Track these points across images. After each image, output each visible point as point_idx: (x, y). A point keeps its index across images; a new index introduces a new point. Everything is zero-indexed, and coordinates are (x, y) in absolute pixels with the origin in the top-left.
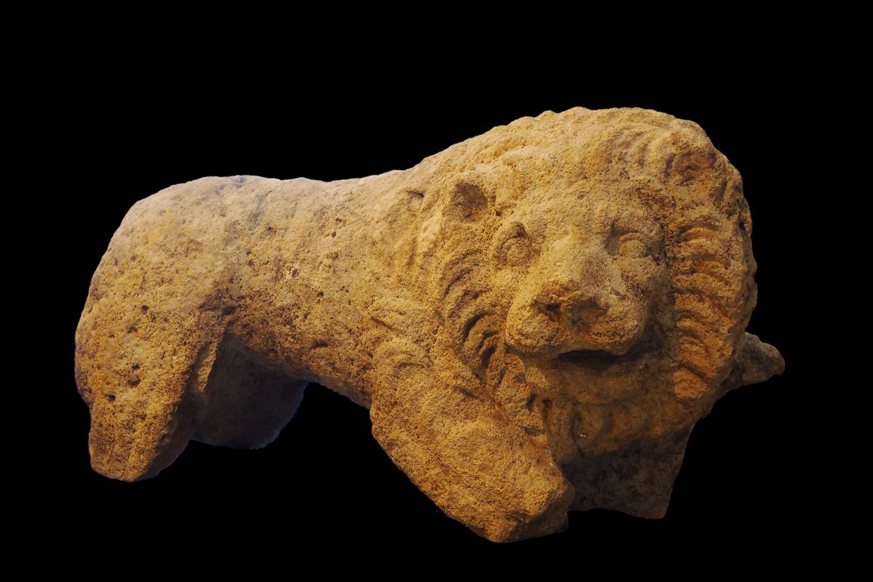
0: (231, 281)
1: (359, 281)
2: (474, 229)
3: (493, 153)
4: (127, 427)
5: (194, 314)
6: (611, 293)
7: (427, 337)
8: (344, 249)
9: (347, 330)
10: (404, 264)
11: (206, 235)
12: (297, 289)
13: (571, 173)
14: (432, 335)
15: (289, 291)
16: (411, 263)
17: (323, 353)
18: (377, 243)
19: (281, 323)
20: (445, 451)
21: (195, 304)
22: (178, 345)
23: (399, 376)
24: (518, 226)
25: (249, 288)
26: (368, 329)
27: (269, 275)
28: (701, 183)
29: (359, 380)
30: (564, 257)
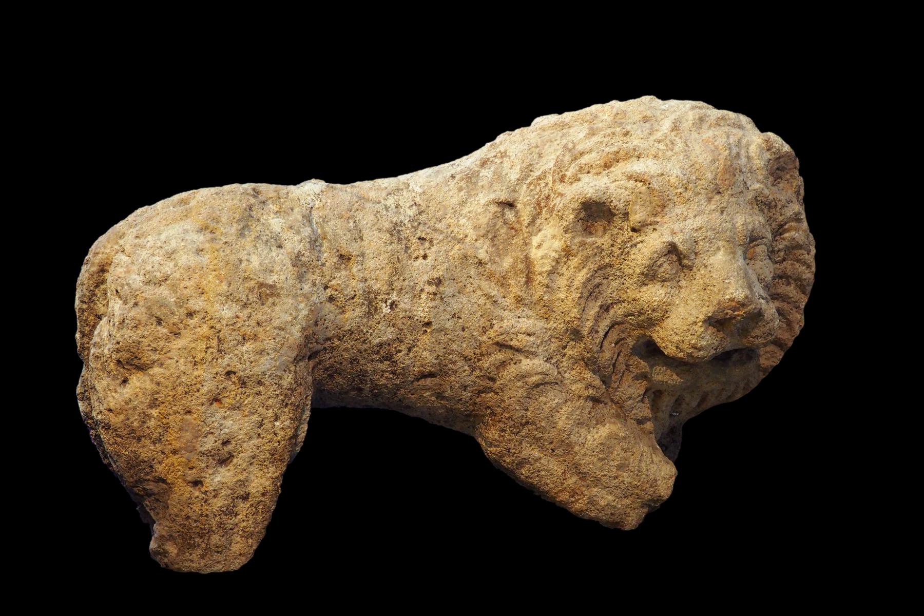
0: (316, 324)
1: (470, 306)
2: (599, 244)
3: (603, 164)
4: (227, 512)
5: (290, 370)
6: (759, 299)
7: (555, 354)
8: (445, 273)
9: (462, 358)
10: (522, 283)
11: (272, 274)
12: (399, 322)
13: (706, 189)
14: (562, 350)
15: (389, 326)
16: (529, 281)
17: (430, 385)
18: (487, 264)
19: (378, 360)
20: (584, 459)
21: (289, 359)
22: (279, 409)
23: (531, 396)
24: (669, 245)
25: (337, 328)
26: (489, 354)
27: (358, 312)
28: (786, 182)
29: (470, 405)
30: (730, 275)
